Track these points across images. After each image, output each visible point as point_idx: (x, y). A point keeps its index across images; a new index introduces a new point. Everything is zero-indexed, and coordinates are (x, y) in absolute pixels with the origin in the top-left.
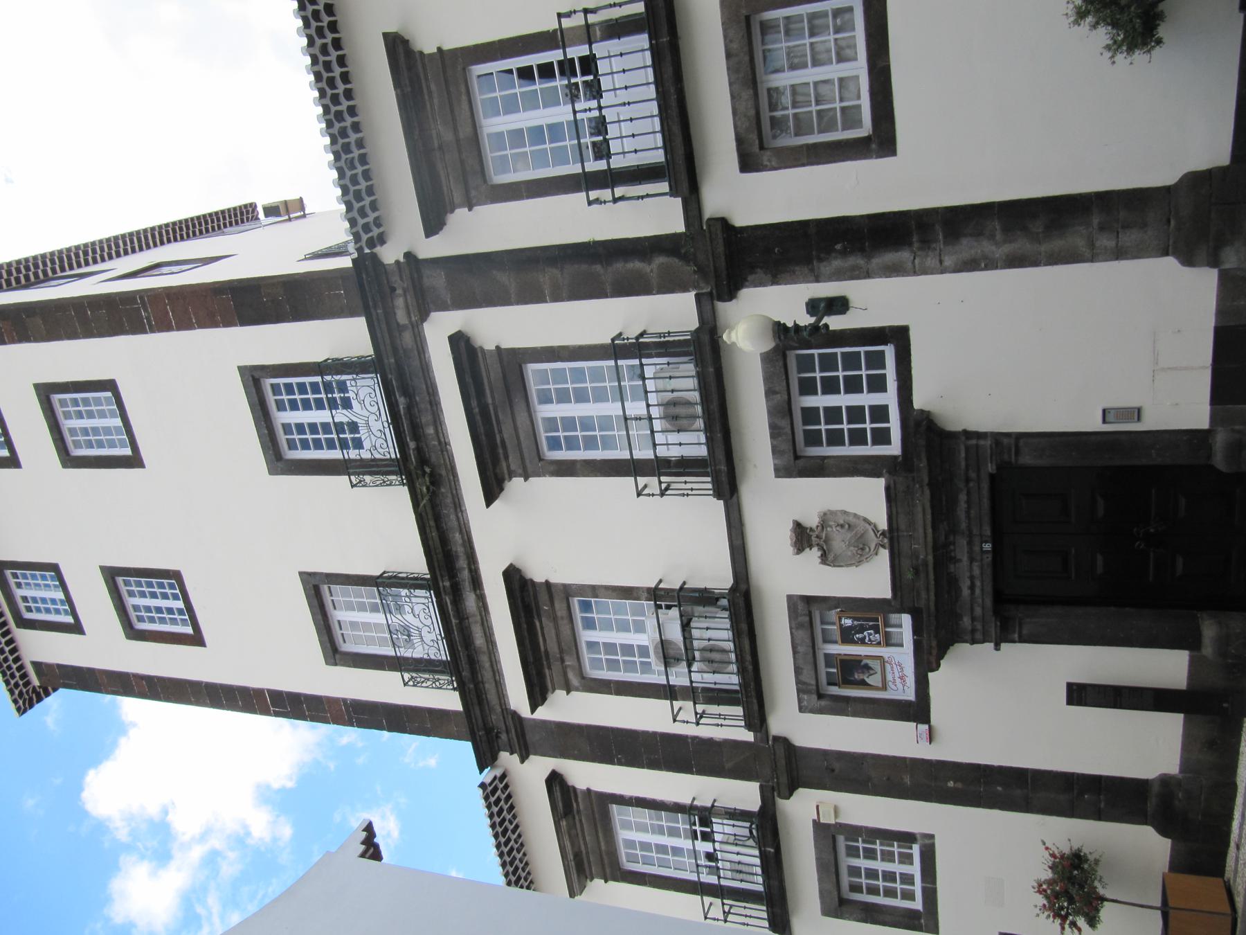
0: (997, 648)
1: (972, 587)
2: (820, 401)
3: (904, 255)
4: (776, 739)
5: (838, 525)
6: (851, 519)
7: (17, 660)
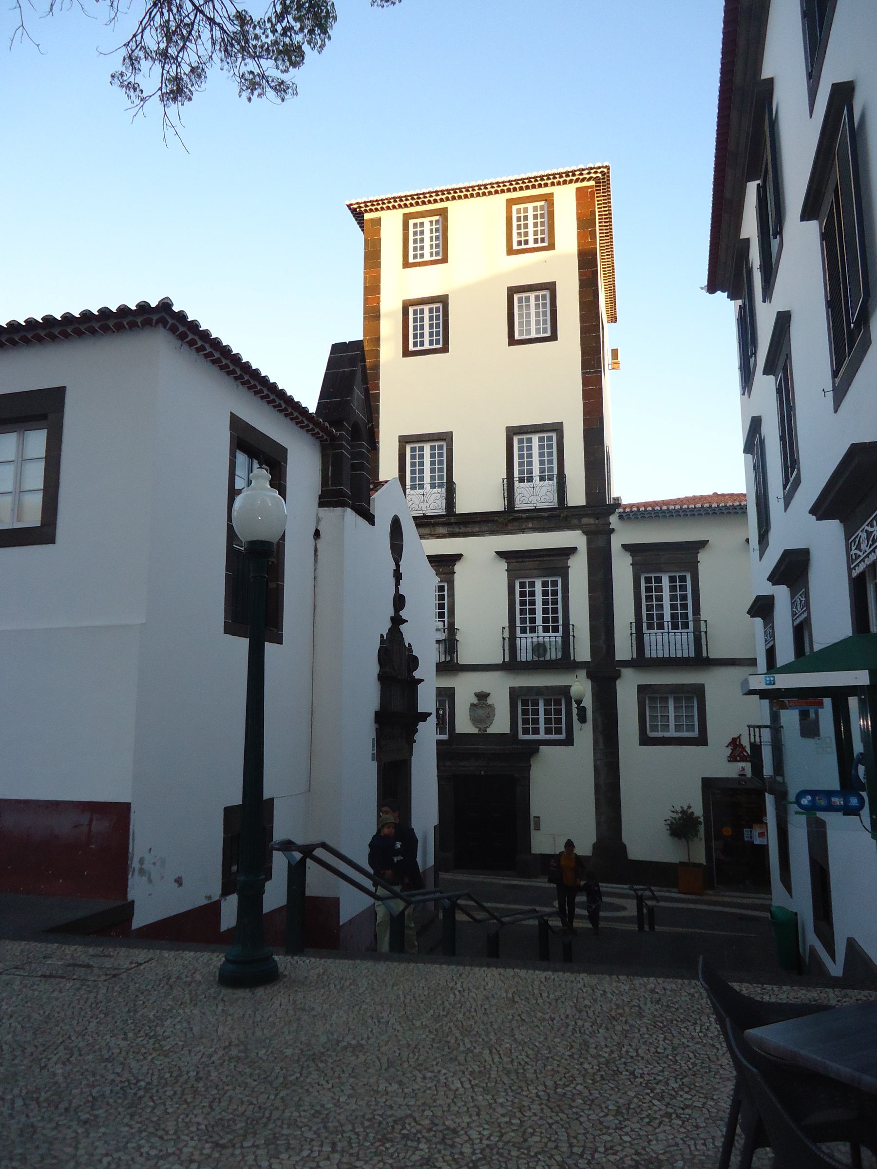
2: (541, 708)
3: (602, 746)
7: (382, 209)
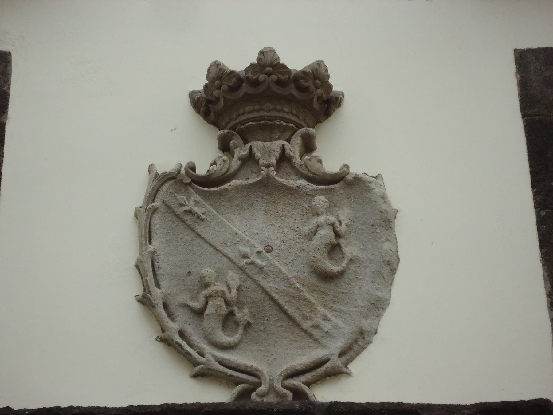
5: (337, 235)
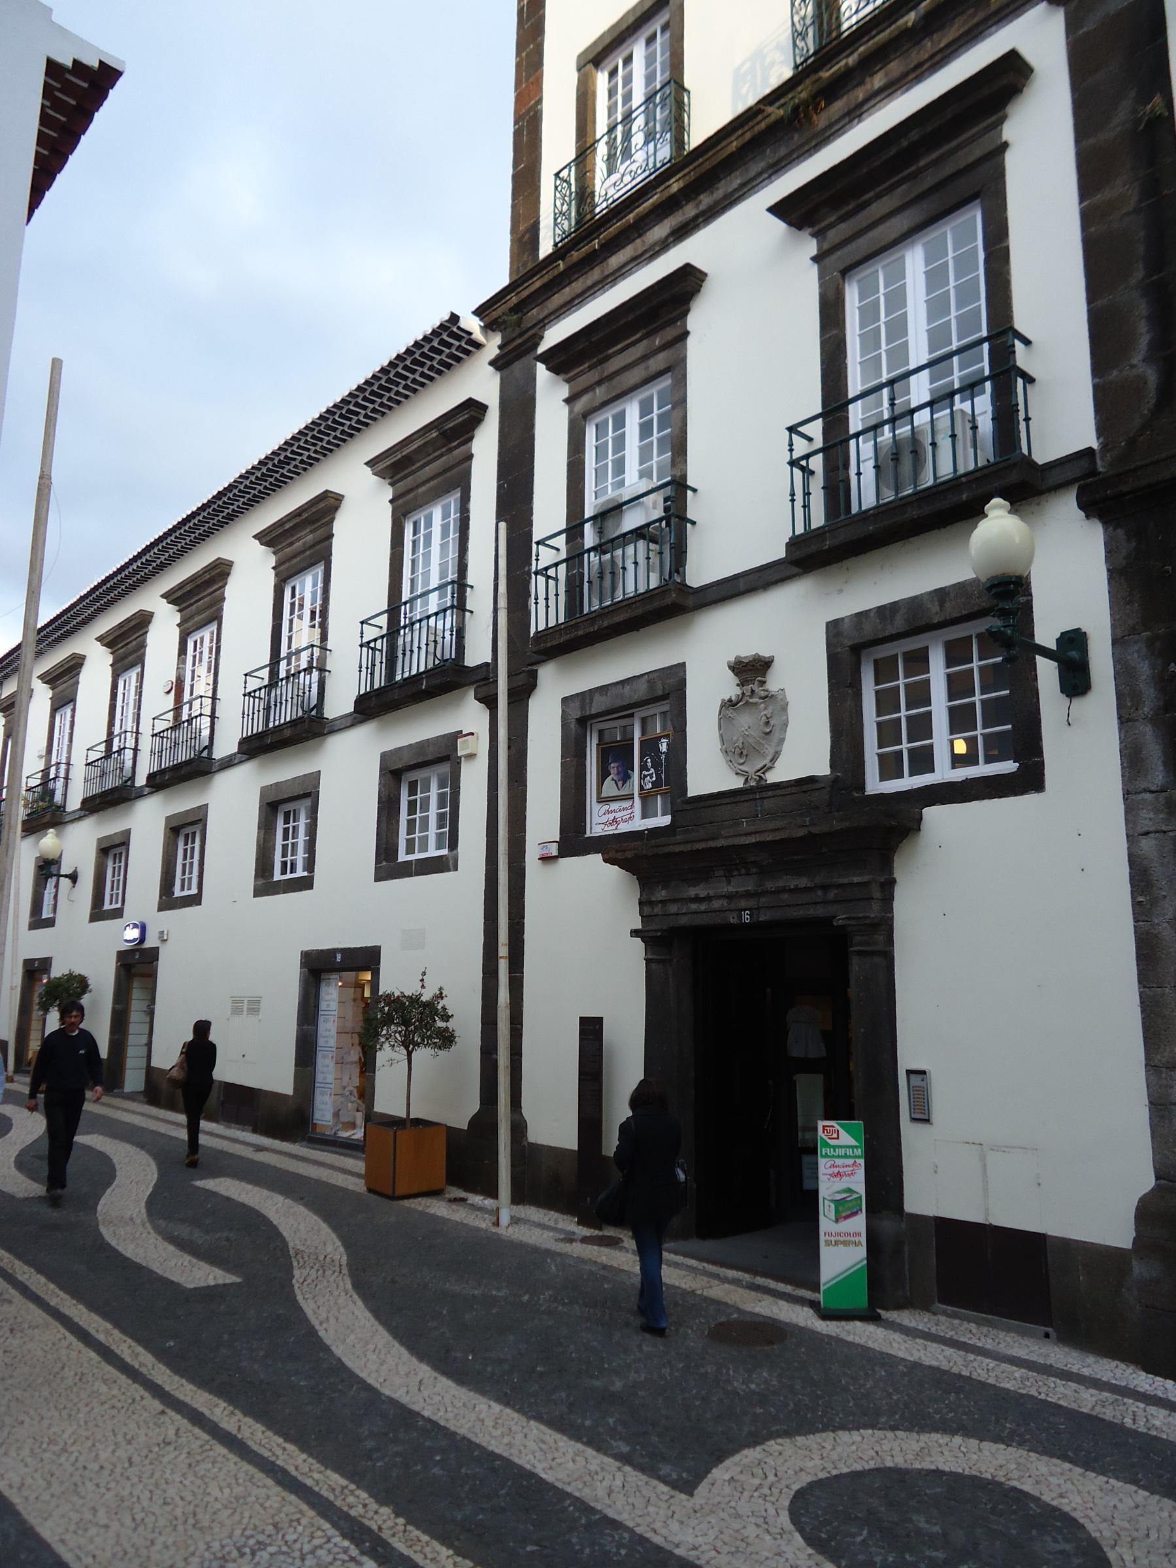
0: (635, 933)
1: (697, 899)
3: (1158, 776)
4: (534, 676)
6: (776, 735)
